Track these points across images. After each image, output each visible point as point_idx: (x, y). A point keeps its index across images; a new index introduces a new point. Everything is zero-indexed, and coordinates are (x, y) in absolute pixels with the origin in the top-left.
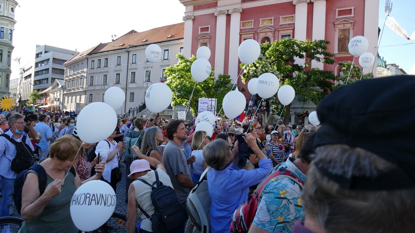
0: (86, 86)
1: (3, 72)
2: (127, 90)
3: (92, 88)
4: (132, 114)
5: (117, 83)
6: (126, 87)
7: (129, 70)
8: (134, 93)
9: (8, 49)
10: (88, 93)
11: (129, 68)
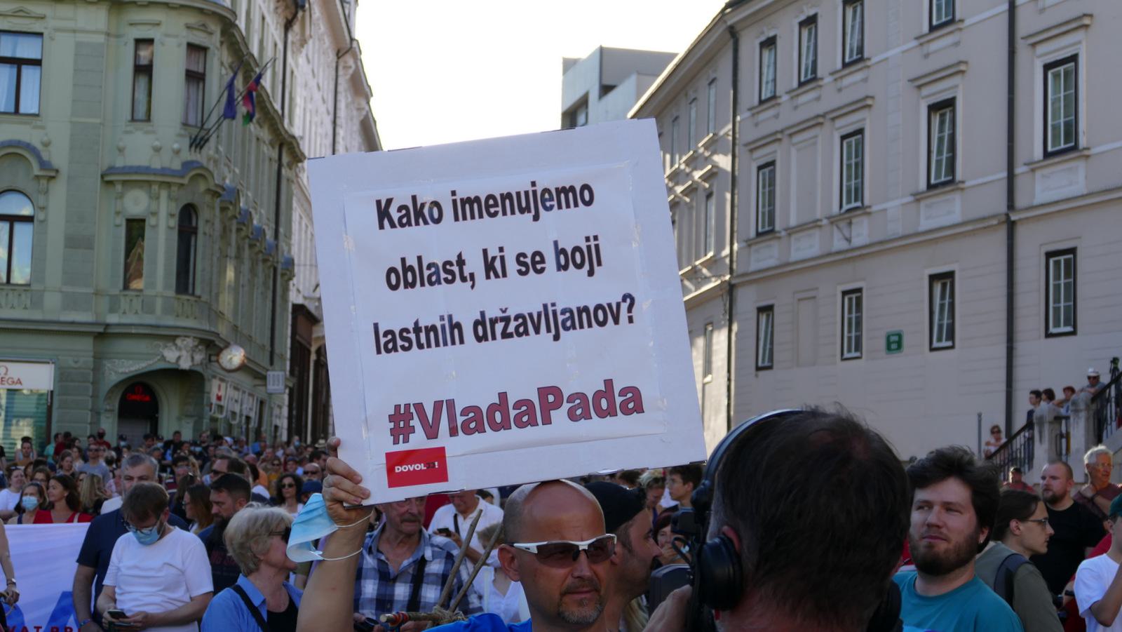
0: (736, 246)
1: (155, 188)
2: (1022, 233)
3: (768, 255)
4: (1046, 445)
5: (936, 186)
6: (1003, 208)
7: (1021, 46)
8: (1073, 251)
9: (188, 27)
10: (748, 300)
11: (1022, 29)
